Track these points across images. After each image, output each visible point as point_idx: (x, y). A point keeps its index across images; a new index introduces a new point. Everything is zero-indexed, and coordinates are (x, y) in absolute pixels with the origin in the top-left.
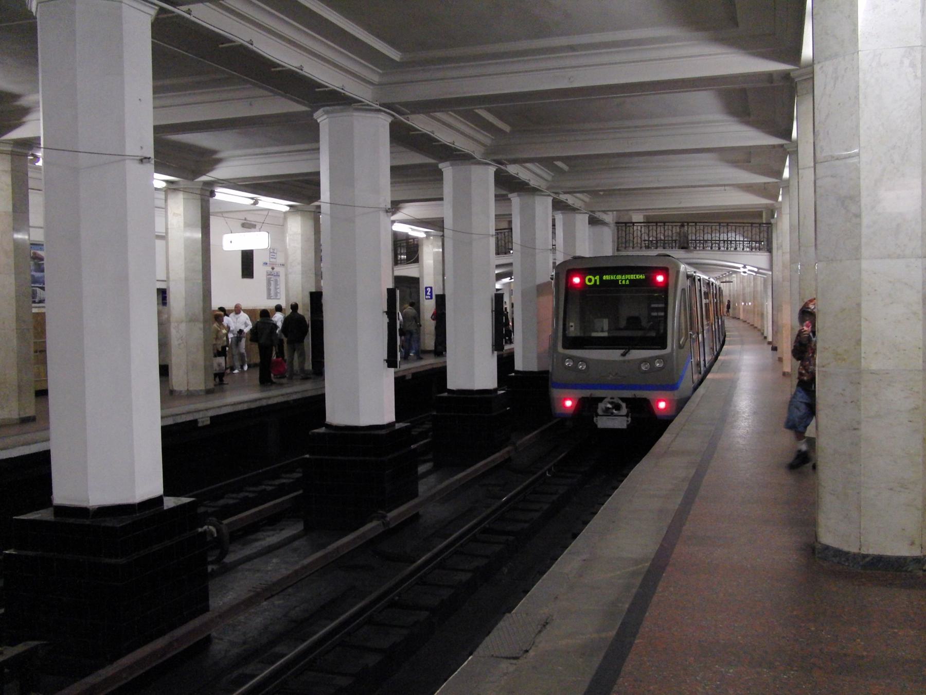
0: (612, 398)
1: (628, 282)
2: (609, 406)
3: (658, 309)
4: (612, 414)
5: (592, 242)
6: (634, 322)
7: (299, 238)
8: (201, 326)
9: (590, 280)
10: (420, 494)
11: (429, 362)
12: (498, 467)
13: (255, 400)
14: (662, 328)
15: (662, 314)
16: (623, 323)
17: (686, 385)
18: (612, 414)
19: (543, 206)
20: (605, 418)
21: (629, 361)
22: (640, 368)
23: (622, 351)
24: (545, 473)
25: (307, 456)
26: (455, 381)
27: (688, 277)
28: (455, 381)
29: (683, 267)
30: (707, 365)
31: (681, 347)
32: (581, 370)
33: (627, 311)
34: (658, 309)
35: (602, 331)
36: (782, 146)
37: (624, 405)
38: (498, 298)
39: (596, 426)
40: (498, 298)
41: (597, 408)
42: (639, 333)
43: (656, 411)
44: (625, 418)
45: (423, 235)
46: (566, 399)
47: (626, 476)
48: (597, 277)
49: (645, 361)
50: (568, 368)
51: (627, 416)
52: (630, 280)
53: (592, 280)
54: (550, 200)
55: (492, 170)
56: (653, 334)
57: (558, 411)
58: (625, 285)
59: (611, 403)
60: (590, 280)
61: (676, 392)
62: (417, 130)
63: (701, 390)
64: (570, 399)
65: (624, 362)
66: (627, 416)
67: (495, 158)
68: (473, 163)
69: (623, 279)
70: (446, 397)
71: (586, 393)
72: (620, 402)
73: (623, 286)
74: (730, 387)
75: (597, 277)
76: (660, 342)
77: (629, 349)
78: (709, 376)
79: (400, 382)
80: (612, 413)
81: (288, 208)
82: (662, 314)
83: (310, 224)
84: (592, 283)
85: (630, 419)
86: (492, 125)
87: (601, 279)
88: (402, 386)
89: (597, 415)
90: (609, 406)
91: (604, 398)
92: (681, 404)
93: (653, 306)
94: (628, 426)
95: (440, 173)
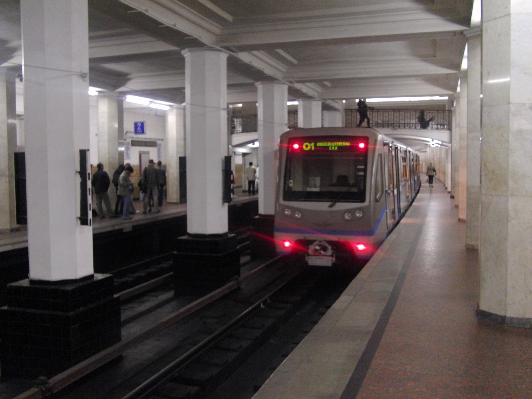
0: (320, 242)
1: (336, 148)
2: (318, 248)
3: (361, 170)
4: (320, 254)
5: (313, 118)
6: (343, 180)
7: (106, 115)
8: (7, 179)
9: (307, 146)
10: (123, 339)
11: (170, 211)
12: (225, 297)
13: (101, 228)
14: (362, 184)
15: (362, 173)
16: (335, 181)
17: (381, 230)
18: (320, 254)
19: (281, 91)
20: (314, 257)
21: (335, 212)
22: (343, 216)
23: (329, 203)
24: (259, 305)
25: (5, 308)
26: (194, 227)
27: (385, 144)
28: (194, 227)
29: (380, 137)
30: (402, 211)
31: (377, 201)
32: (297, 219)
33: (340, 170)
34: (361, 170)
35: (315, 187)
36: (461, 33)
37: (329, 247)
38: (228, 160)
39: (307, 263)
40: (228, 160)
41: (308, 249)
42: (344, 189)
43: (355, 251)
44: (330, 258)
45: (167, 108)
46: (285, 241)
47: (273, 369)
48: (313, 144)
49: (348, 211)
50: (286, 216)
51: (332, 256)
52: (339, 147)
53: (308, 146)
54: (285, 88)
55: (223, 57)
56: (355, 190)
57: (279, 249)
58: (334, 151)
59: (319, 245)
60: (307, 146)
61: (372, 237)
62: (134, 9)
63: (393, 235)
64: (289, 241)
65: (331, 212)
66: (332, 256)
67: (227, 44)
68: (206, 50)
69: (333, 146)
70: (184, 240)
71: (301, 236)
72: (327, 245)
73: (332, 151)
74: (419, 231)
75: (313, 144)
76: (360, 197)
77: (335, 202)
78: (403, 221)
79: (97, 238)
80: (320, 254)
81: (97, 93)
82: (362, 173)
83: (115, 104)
84: (309, 148)
85: (334, 259)
86: (210, 10)
87: (315, 146)
88: (100, 242)
89: (308, 255)
90: (318, 248)
91: (315, 241)
92: (378, 245)
93: (358, 167)
94: (333, 264)
95: (182, 59)
